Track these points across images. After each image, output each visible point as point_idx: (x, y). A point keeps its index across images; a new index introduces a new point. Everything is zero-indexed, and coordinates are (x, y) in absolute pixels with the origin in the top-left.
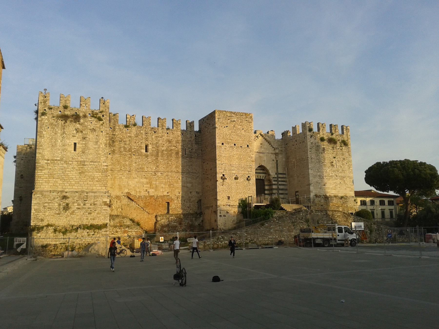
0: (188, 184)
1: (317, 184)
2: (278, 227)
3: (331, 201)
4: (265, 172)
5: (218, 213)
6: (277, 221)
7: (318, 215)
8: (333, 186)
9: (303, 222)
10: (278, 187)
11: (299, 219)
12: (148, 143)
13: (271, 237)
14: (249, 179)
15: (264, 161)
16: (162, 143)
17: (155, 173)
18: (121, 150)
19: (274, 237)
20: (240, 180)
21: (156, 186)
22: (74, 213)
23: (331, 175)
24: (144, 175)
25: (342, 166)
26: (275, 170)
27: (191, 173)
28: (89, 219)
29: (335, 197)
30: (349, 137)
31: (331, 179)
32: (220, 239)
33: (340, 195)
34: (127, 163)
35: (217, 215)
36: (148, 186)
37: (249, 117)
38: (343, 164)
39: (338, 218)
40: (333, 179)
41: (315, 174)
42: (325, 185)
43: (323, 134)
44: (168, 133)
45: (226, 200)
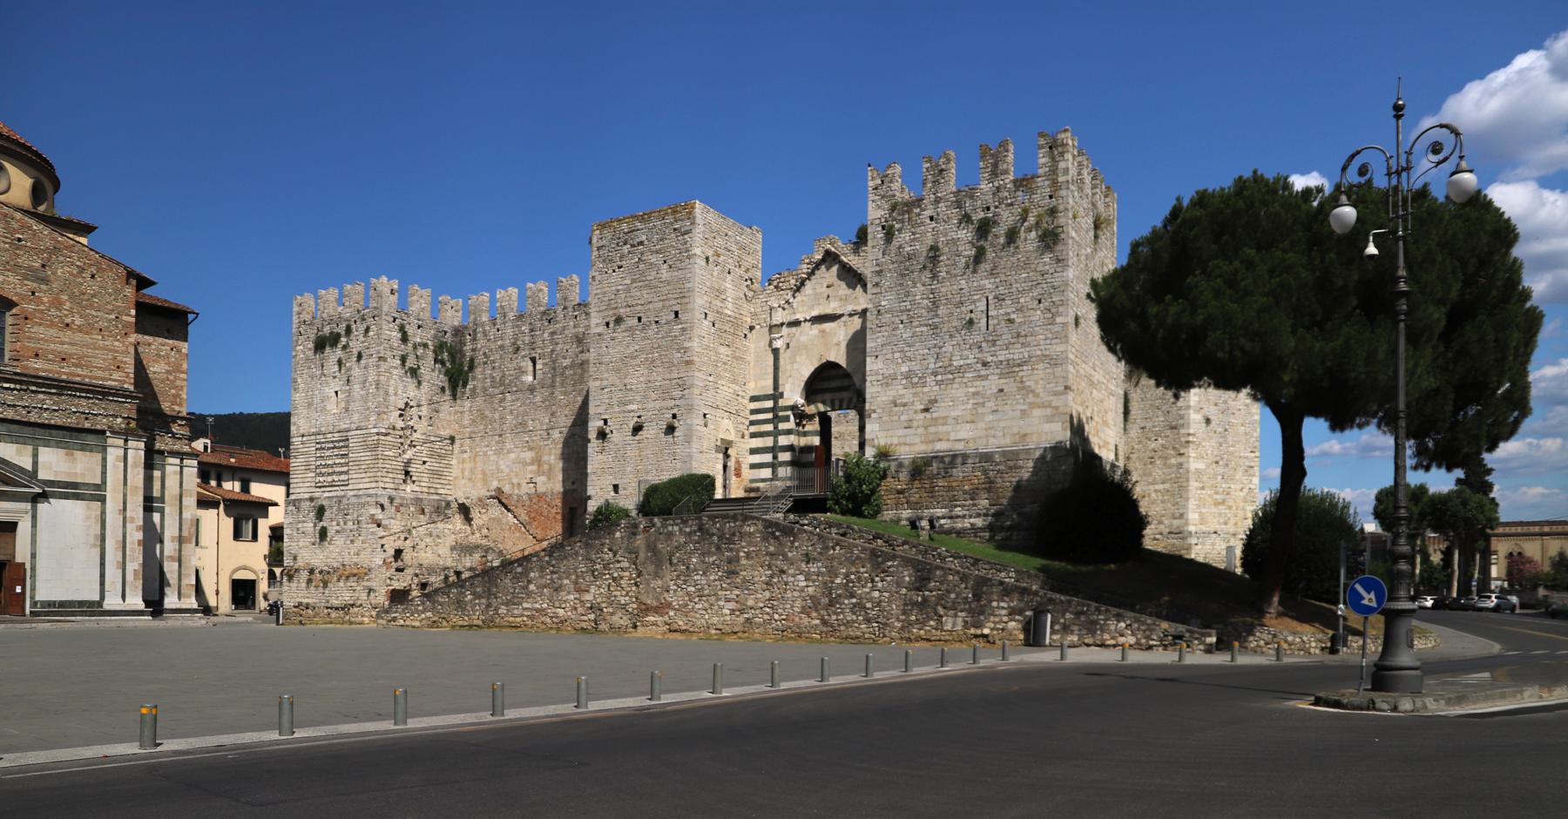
1: (897, 409)
6: (547, 558)
12: (533, 355)
13: (529, 606)
16: (563, 349)
17: (548, 434)
18: (486, 385)
19: (537, 606)
20: (652, 432)
21: (550, 469)
22: (333, 542)
23: (962, 362)
24: (528, 442)
28: (352, 553)
31: (957, 380)
32: (418, 605)
34: (497, 416)
36: (534, 468)
39: (744, 544)
40: (965, 380)
42: (926, 410)
44: (576, 317)
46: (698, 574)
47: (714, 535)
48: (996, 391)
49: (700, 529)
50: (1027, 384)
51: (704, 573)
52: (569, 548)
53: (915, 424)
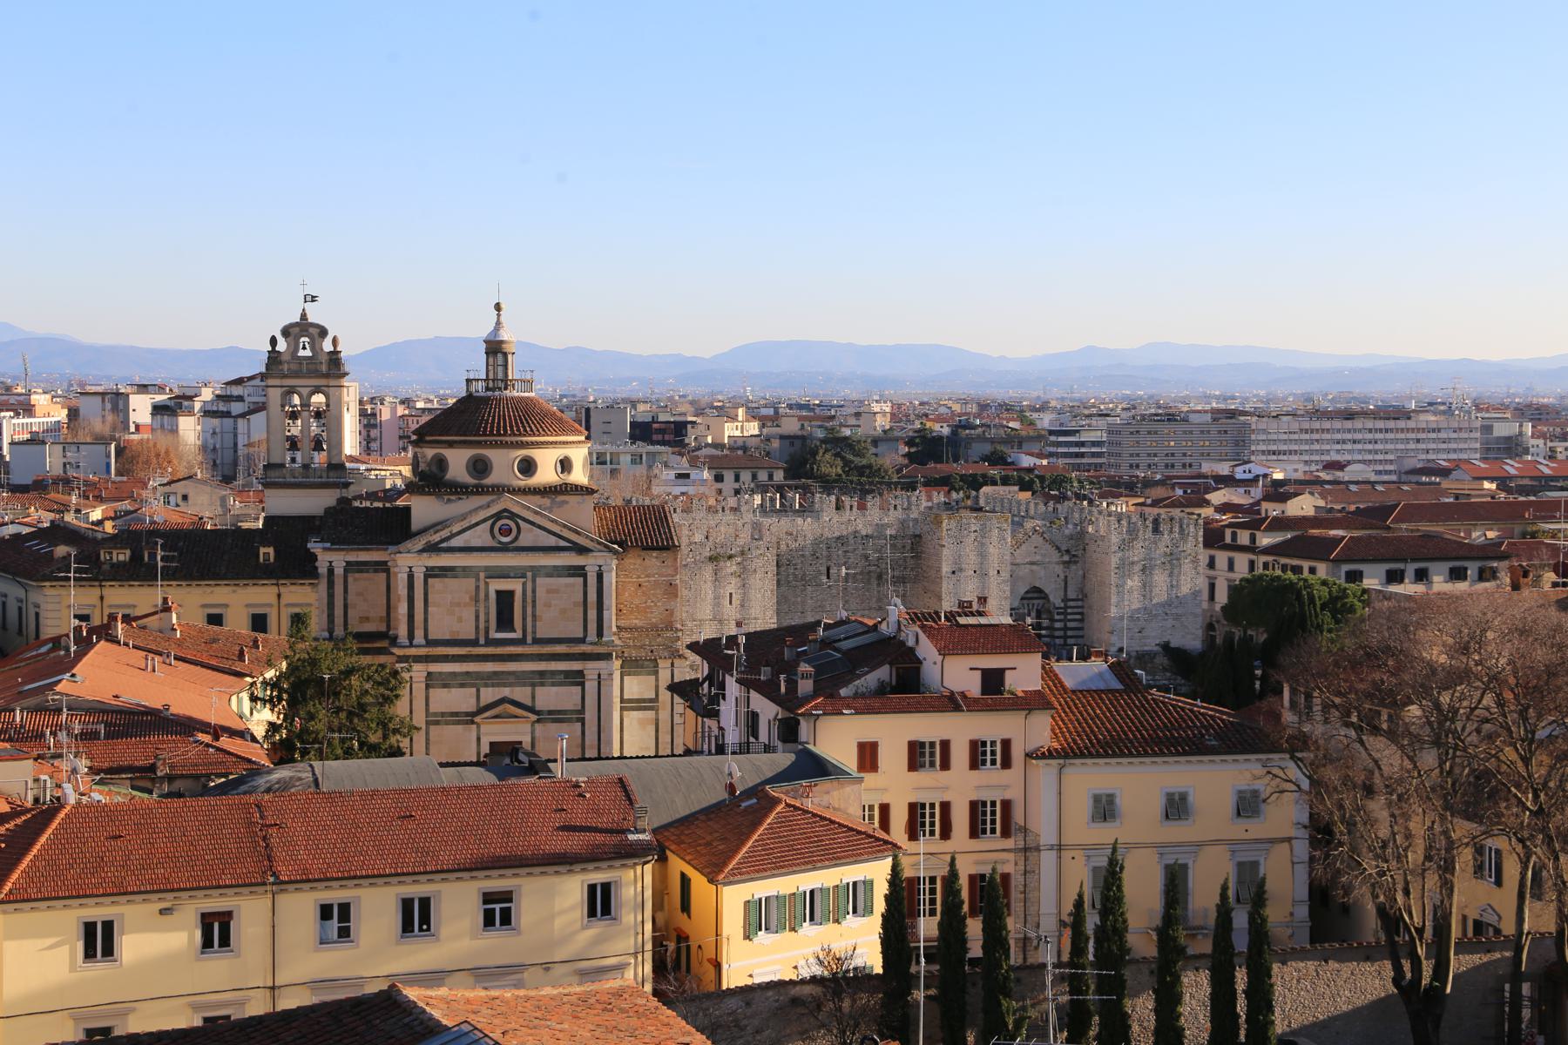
4: (1043, 595)
10: (1065, 625)
15: (1040, 578)
26: (1062, 594)
34: (799, 599)
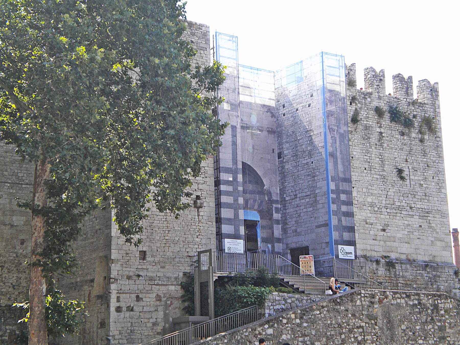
0: (14, 218)
2: (300, 339)
3: (401, 274)
5: (112, 300)
6: (298, 321)
7: (399, 306)
8: (404, 232)
9: (363, 324)
11: (354, 315)
14: (199, 205)
25: (422, 183)
27: (27, 184)
29: (410, 262)
30: (437, 110)
31: (398, 215)
33: (422, 257)
35: (108, 306)
37: (199, 35)
38: (425, 179)
41: (361, 200)
42: (384, 230)
43: (380, 98)
45: (136, 262)
46: (421, 339)
47: (429, 308)
48: (418, 226)
49: (420, 304)
50: (432, 225)
51: (425, 338)
52: (318, 312)
53: (378, 238)
